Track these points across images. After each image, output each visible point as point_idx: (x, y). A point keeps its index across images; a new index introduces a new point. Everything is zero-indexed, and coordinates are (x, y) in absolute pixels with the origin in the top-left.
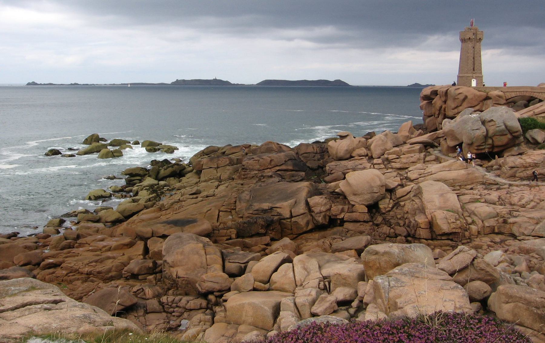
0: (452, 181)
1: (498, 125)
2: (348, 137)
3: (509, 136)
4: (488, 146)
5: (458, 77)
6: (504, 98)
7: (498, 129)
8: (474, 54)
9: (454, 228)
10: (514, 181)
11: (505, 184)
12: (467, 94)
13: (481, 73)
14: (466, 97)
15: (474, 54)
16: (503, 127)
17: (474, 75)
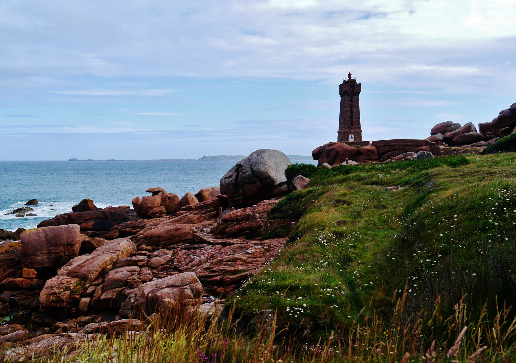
0: (156, 239)
1: (244, 171)
2: (160, 193)
3: (258, 184)
4: (241, 198)
5: (339, 132)
6: (376, 152)
7: (244, 175)
8: (352, 108)
9: (53, 301)
10: (222, 239)
11: (206, 242)
12: (338, 150)
13: (359, 128)
14: (338, 152)
15: (352, 108)
16: (250, 172)
17: (352, 131)
